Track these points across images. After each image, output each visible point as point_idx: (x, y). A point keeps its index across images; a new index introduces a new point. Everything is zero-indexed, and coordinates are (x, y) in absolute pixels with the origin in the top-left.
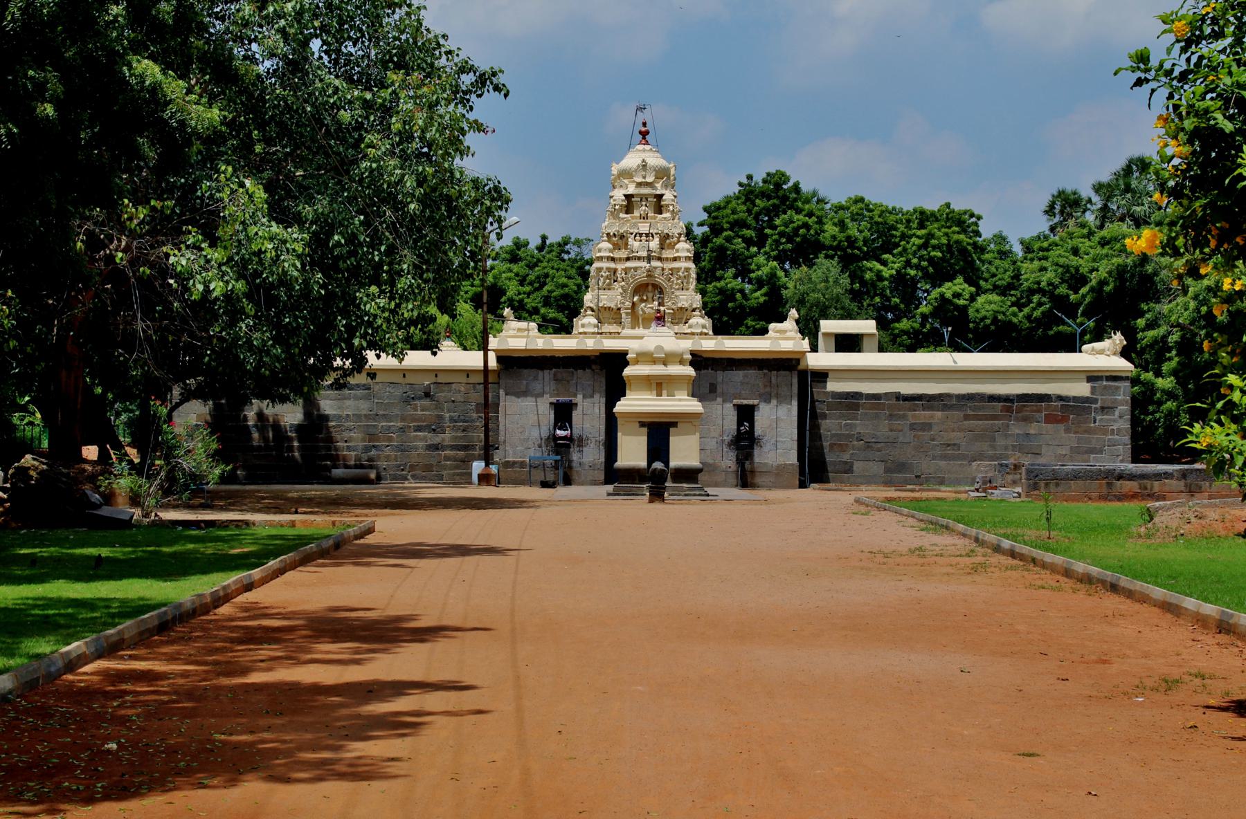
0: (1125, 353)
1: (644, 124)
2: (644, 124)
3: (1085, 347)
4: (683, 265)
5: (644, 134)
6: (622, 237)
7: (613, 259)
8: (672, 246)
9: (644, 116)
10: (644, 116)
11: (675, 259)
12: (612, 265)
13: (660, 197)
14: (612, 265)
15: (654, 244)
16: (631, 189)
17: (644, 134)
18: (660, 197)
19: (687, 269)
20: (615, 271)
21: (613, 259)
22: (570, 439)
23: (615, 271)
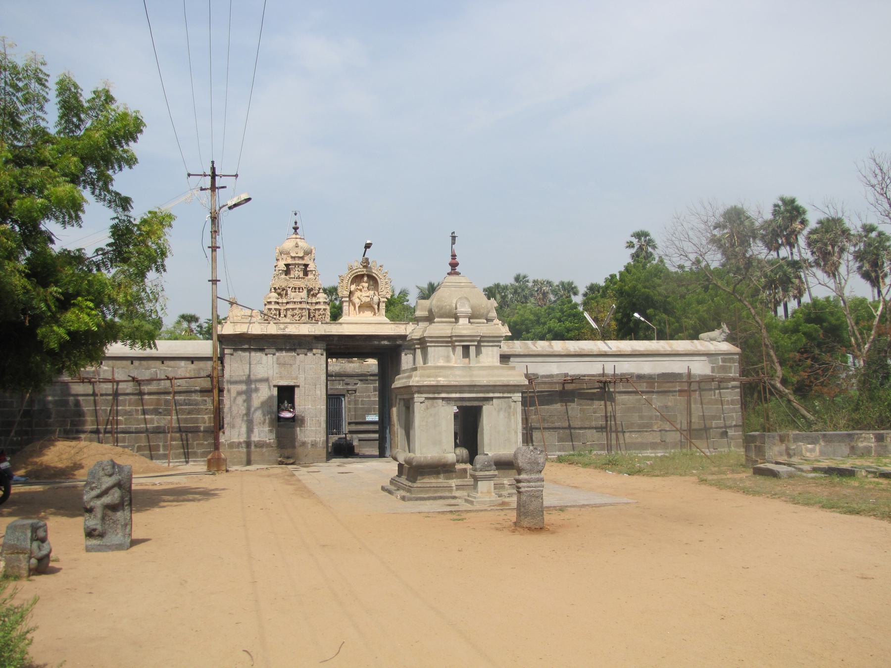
0: (730, 339)
1: (296, 223)
2: (296, 223)
3: (701, 336)
4: (322, 307)
5: (296, 229)
6: (283, 290)
7: (278, 303)
8: (315, 295)
9: (297, 218)
10: (297, 218)
11: (317, 303)
12: (277, 307)
13: (306, 266)
14: (277, 307)
15: (304, 294)
16: (290, 261)
17: (296, 229)
18: (306, 266)
19: (325, 310)
20: (279, 310)
21: (278, 303)
22: (293, 419)
23: (279, 310)
